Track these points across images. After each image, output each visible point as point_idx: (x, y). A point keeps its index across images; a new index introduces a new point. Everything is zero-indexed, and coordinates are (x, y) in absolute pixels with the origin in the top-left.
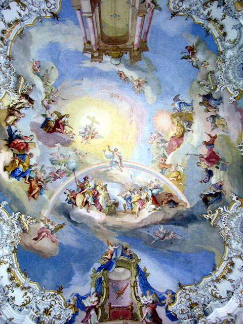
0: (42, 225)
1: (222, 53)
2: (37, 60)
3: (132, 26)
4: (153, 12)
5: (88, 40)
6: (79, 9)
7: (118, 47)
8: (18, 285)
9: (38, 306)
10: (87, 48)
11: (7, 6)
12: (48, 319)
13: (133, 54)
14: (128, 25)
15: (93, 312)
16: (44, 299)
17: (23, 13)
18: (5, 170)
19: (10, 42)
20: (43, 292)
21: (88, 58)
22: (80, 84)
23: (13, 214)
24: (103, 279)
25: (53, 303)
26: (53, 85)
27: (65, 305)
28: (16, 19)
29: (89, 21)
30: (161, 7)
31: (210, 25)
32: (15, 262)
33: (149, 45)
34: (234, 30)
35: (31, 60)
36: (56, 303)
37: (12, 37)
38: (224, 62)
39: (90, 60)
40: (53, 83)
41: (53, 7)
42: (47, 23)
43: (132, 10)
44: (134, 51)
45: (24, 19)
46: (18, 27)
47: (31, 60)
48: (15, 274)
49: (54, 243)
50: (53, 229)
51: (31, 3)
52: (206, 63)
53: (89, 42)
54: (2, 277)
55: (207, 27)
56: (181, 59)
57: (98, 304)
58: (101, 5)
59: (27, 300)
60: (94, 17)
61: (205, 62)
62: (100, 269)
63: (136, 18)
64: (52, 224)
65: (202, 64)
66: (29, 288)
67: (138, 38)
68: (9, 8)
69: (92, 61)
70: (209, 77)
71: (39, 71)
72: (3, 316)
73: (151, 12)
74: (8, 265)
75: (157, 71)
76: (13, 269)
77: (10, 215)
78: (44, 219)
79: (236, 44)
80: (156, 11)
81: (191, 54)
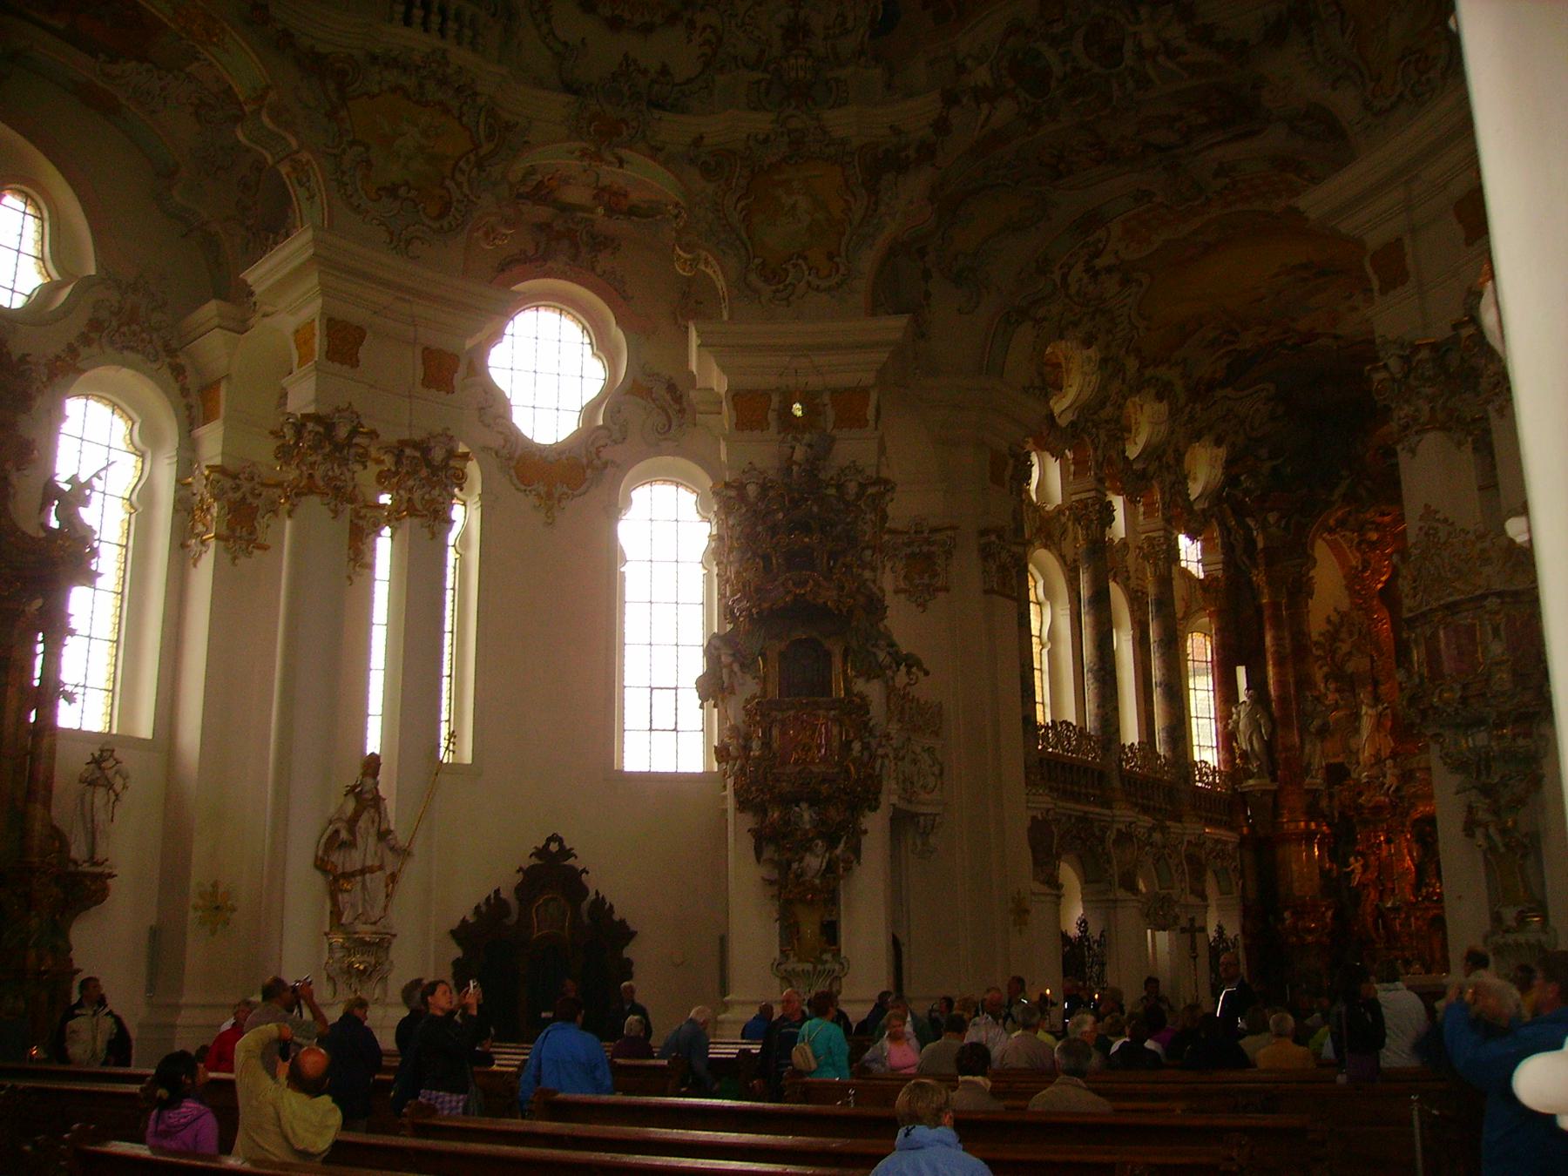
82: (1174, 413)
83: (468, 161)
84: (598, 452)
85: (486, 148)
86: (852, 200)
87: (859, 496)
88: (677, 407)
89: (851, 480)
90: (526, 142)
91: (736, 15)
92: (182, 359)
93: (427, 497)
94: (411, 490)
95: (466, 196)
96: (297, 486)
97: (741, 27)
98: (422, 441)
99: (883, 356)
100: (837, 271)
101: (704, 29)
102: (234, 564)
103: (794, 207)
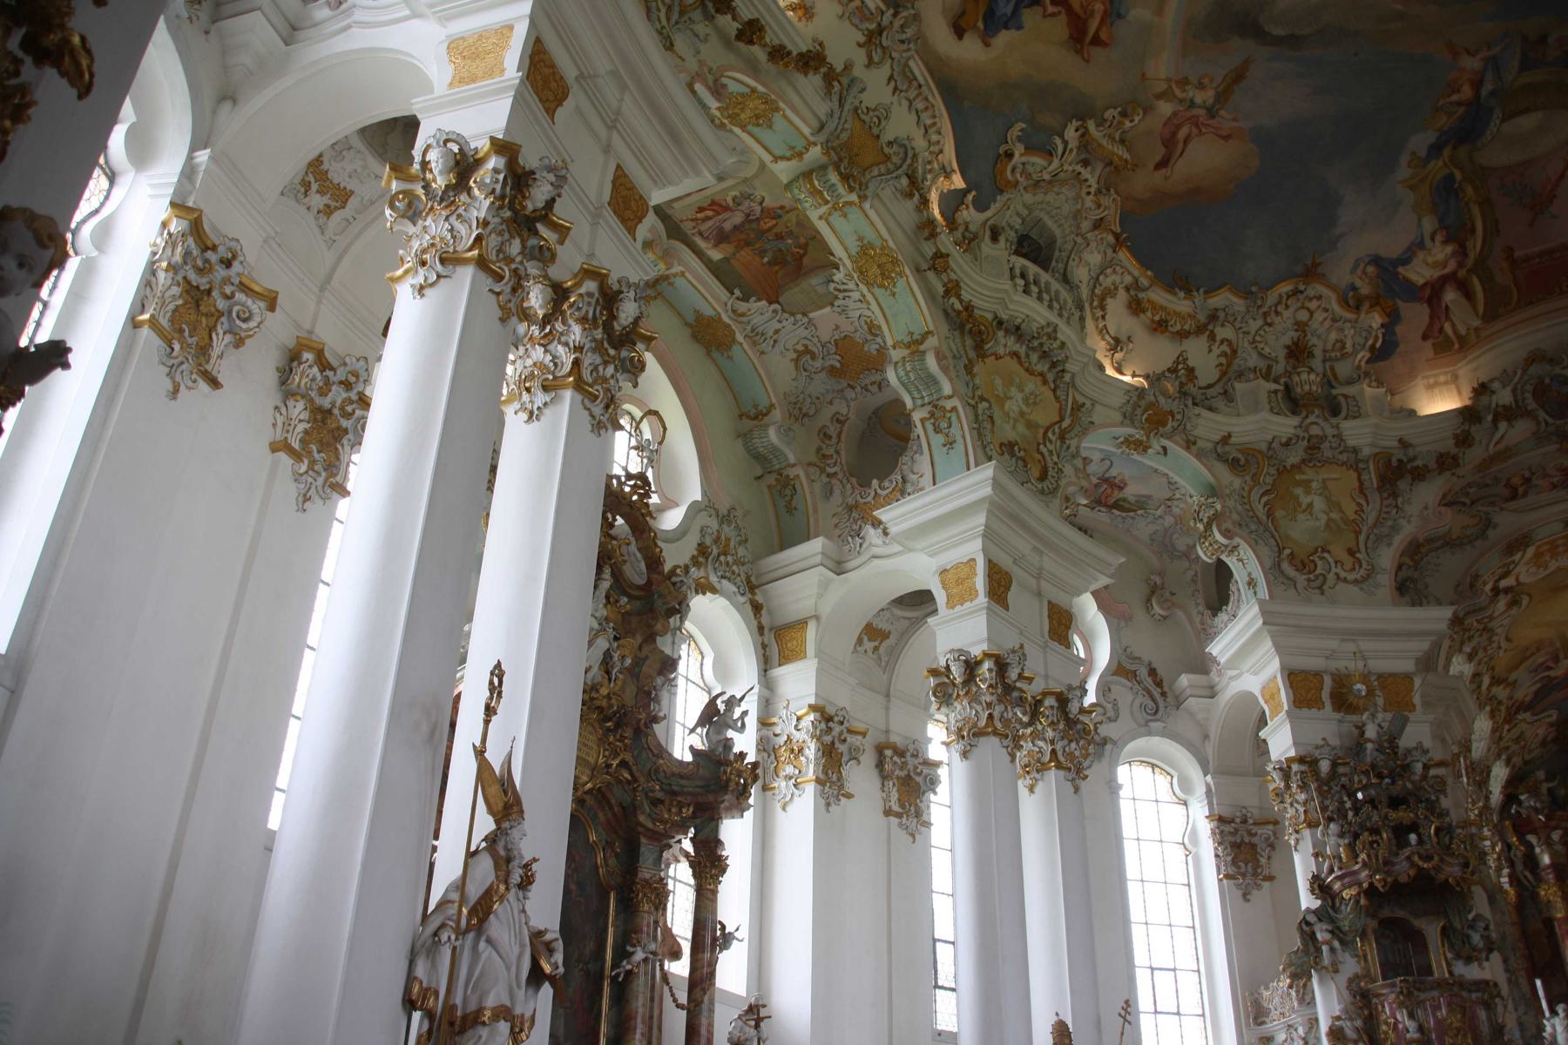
0: (1166, 108)
8: (1183, 335)
9: (1267, 350)
12: (1318, 379)
15: (1450, 296)
16: (1269, 320)
18: (959, 32)
20: (1259, 303)
23: (1058, 141)
24: (1458, 176)
25: (1303, 316)
27: (1344, 302)
32: (1136, 273)
36: (1311, 313)
48: (1155, 307)
49: (1230, 141)
50: (1211, 101)
54: (1129, 338)
57: (1460, 265)
59: (1224, 354)
62: (1435, 149)
64: (1201, 86)
66: (1213, 317)
72: (1200, 444)
74: (1122, 295)
76: (1141, 295)
77: (1050, 154)
78: (1164, 86)
82: (1494, 731)
83: (1054, 433)
84: (1096, 729)
85: (1065, 424)
86: (1365, 505)
87: (1424, 777)
88: (1159, 690)
89: (1418, 761)
90: (1092, 423)
91: (1248, 333)
92: (759, 598)
93: (1067, 749)
94: (1052, 742)
95: (1056, 463)
96: (975, 725)
97: (1252, 343)
98: (1061, 693)
99: (1423, 645)
100: (1361, 567)
101: (1222, 342)
102: (828, 811)
103: (1310, 505)
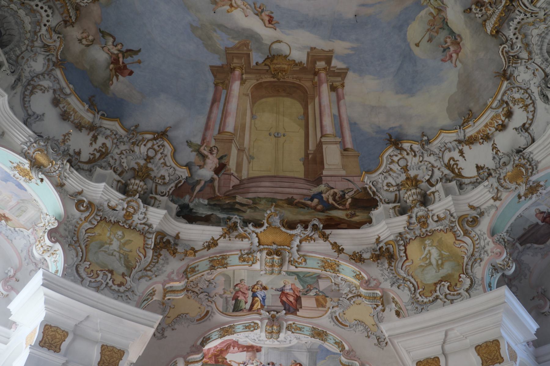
1: (55, 64)
2: (448, 64)
3: (245, 114)
4: (204, 139)
5: (334, 94)
6: (346, 150)
7: (273, 77)
10: (339, 79)
11: (481, 171)
13: (243, 61)
14: (253, 117)
17: (456, 155)
19: (494, 105)
21: (338, 58)
22: (363, 5)
26: (422, 7)
28: (472, 146)
29: (329, 128)
30: (188, 147)
31: (88, 117)
33: (210, 77)
34: (39, 112)
35: (459, 65)
37: (486, 117)
38: (46, 47)
39: (334, 55)
40: (423, 13)
41: (396, 159)
42: (412, 130)
43: (243, 144)
44: (241, 68)
45: (454, 143)
46: (471, 131)
47: (459, 65)
51: (436, 170)
52: (84, 42)
53: (333, 88)
55: (94, 115)
56: (139, 51)
58: (303, 155)
60: (319, 135)
61: (88, 46)
63: (235, 129)
65: (93, 41)
67: (232, 92)
68: (478, 168)
69: (331, 51)
70: (72, 13)
71: (448, 40)
73: (208, 139)
75: (191, 26)
79: (29, 84)
80: (197, 140)
81: (121, 60)
